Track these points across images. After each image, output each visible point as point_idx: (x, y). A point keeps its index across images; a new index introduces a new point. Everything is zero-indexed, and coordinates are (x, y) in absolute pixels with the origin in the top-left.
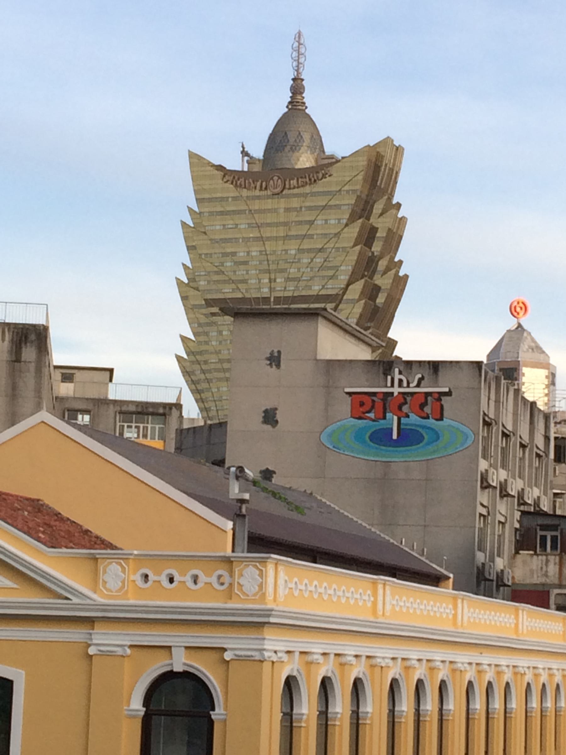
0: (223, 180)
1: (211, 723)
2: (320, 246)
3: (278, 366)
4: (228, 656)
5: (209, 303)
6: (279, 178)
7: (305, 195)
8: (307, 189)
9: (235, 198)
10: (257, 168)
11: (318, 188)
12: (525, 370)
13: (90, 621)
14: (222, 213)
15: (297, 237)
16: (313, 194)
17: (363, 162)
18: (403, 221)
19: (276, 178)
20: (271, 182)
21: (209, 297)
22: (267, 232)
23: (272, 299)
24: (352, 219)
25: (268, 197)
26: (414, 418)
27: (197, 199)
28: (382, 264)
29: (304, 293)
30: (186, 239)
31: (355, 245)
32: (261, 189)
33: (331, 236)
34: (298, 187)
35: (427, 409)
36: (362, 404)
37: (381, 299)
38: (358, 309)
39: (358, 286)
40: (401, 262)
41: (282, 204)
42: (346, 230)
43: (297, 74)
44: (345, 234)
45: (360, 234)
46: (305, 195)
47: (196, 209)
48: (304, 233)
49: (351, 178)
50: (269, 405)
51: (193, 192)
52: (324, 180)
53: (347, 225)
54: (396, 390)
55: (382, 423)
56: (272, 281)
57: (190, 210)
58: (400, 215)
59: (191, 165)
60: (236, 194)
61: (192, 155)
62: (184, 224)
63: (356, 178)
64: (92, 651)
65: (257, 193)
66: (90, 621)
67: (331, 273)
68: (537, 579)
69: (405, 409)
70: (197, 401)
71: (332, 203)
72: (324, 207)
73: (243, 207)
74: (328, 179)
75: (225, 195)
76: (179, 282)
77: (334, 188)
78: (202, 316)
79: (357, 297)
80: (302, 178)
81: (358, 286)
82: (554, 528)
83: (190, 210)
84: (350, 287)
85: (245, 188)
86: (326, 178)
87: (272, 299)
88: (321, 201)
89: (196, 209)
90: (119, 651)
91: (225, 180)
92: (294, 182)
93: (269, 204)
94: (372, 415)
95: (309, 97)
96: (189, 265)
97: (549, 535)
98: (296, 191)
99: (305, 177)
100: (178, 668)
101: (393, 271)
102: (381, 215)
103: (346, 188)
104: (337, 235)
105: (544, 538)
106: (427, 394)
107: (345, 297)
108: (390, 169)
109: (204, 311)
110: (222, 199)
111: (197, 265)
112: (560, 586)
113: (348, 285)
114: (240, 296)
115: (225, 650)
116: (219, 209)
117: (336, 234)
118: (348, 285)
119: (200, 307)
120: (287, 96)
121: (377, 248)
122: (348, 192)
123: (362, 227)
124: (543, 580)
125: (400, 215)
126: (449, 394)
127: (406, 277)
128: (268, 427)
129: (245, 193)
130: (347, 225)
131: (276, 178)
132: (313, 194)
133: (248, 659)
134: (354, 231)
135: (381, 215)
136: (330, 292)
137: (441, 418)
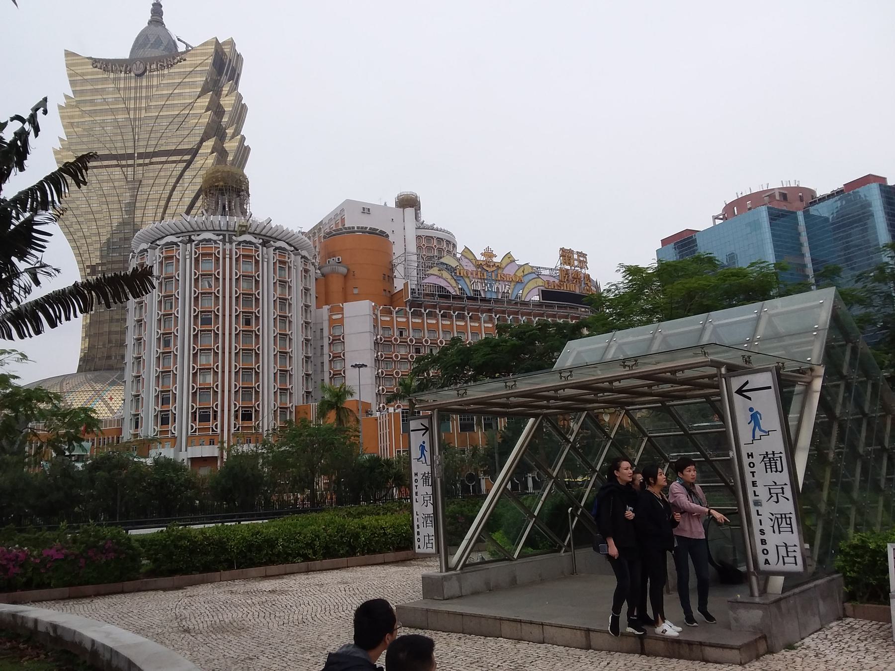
0: (93, 65)
2: (177, 113)
6: (141, 62)
7: (163, 75)
8: (166, 72)
16: (169, 74)
17: (211, 49)
19: (138, 63)
20: (134, 65)
23: (136, 155)
29: (163, 148)
32: (125, 73)
33: (186, 105)
39: (210, 144)
46: (163, 75)
48: (163, 103)
51: (69, 82)
52: (179, 63)
53: (199, 97)
56: (136, 141)
61: (68, 54)
63: (206, 61)
65: (122, 75)
70: (69, 241)
74: (183, 63)
79: (210, 151)
80: (161, 62)
83: (67, 97)
84: (204, 144)
85: (112, 72)
86: (181, 62)
87: (136, 155)
91: (94, 65)
92: (154, 66)
95: (165, 19)
98: (155, 73)
99: (163, 62)
102: (227, 95)
103: (198, 69)
108: (233, 80)
111: (69, 130)
114: (107, 152)
120: (148, 16)
129: (112, 75)
130: (199, 97)
131: (138, 63)
134: (205, 101)
135: (227, 95)
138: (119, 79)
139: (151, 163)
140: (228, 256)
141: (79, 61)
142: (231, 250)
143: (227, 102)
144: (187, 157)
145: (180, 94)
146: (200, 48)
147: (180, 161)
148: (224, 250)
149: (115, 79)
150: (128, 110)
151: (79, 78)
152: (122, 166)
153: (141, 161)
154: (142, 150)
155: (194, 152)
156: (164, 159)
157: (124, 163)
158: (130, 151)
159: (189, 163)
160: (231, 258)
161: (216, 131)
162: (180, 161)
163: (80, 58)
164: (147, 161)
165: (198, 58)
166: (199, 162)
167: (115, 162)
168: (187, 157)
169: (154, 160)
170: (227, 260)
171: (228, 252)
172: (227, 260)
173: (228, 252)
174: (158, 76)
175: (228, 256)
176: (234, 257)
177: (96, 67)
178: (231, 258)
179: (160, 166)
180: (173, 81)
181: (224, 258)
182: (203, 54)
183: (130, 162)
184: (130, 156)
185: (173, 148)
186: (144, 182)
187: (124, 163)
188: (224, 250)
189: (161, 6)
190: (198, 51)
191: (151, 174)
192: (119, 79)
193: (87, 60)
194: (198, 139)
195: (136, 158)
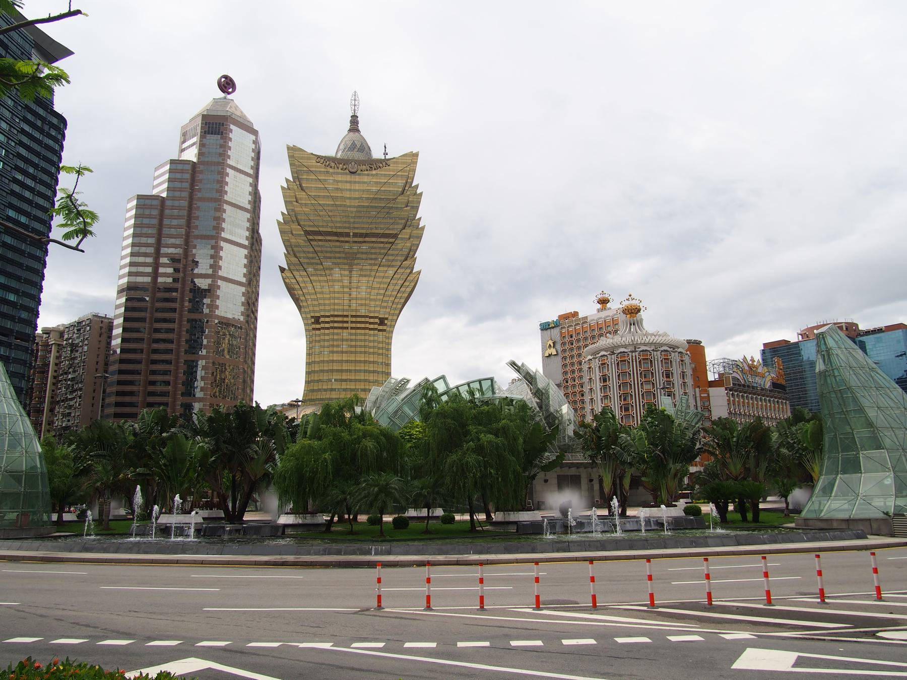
2: (383, 205)
5: (307, 233)
7: (372, 175)
8: (374, 172)
19: (353, 163)
21: (308, 229)
23: (351, 234)
29: (374, 231)
34: (367, 170)
42: (399, 198)
43: (355, 113)
49: (402, 168)
57: (287, 180)
62: (283, 188)
67: (391, 221)
77: (392, 173)
78: (302, 241)
79: (408, 237)
83: (287, 180)
86: (386, 166)
87: (351, 234)
98: (366, 172)
109: (303, 238)
117: (393, 200)
119: (300, 235)
129: (331, 170)
131: (353, 163)
139: (364, 242)
140: (634, 360)
141: (306, 156)
142: (636, 356)
146: (401, 158)
147: (387, 243)
148: (632, 356)
151: (305, 169)
153: (356, 239)
154: (356, 231)
155: (395, 236)
156: (374, 239)
158: (347, 231)
159: (393, 243)
160: (636, 361)
162: (387, 243)
163: (306, 153)
165: (399, 165)
167: (336, 238)
168: (391, 240)
169: (367, 239)
170: (634, 363)
171: (634, 358)
172: (634, 363)
173: (634, 358)
174: (368, 175)
175: (634, 360)
176: (638, 360)
177: (319, 162)
178: (636, 361)
180: (380, 181)
181: (633, 361)
182: (402, 163)
183: (347, 239)
184: (347, 235)
185: (382, 232)
188: (632, 356)
189: (357, 117)
190: (399, 160)
193: (312, 156)
194: (401, 227)
195: (351, 237)
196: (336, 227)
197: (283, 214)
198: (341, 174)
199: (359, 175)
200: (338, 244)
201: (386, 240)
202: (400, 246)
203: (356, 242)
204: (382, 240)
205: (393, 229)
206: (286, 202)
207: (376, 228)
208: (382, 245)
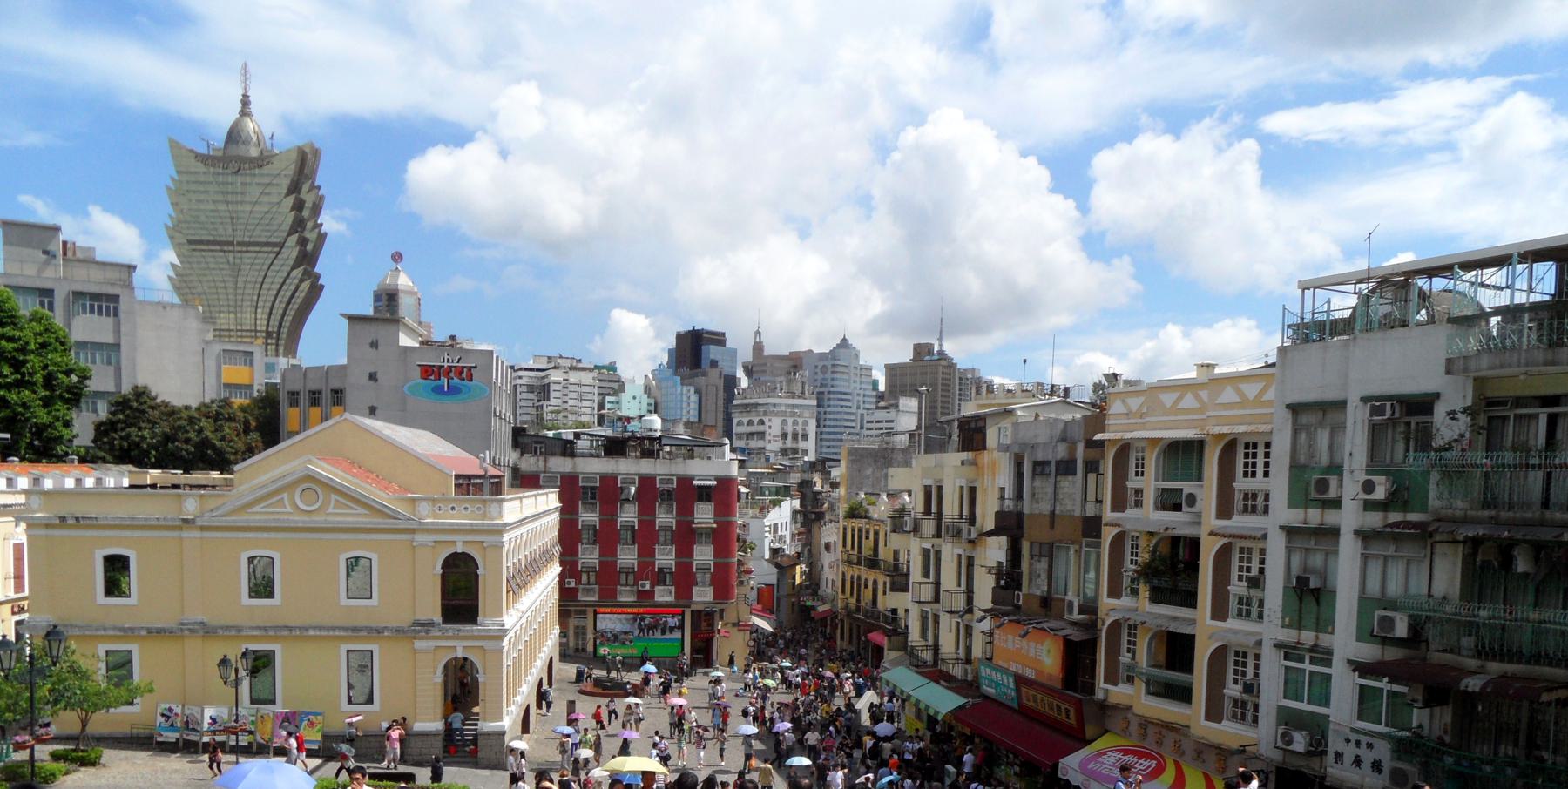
1: (477, 576)
3: (377, 348)
4: (485, 545)
7: (255, 175)
8: (257, 171)
9: (204, 173)
10: (220, 154)
11: (265, 170)
12: (401, 295)
13: (413, 531)
14: (194, 182)
15: (250, 203)
16: (262, 175)
18: (322, 198)
22: (230, 198)
24: (289, 193)
25: (228, 174)
26: (456, 381)
27: (178, 172)
28: (310, 225)
30: (170, 196)
31: (292, 210)
35: (464, 375)
36: (426, 371)
37: (309, 247)
38: (295, 253)
39: (294, 238)
40: (321, 225)
41: (239, 179)
44: (283, 204)
45: (294, 203)
46: (255, 175)
47: (176, 177)
50: (373, 371)
54: (446, 364)
55: (438, 382)
58: (320, 193)
59: (171, 147)
60: (205, 170)
64: (414, 544)
65: (221, 171)
66: (413, 531)
68: (534, 469)
69: (452, 375)
71: (275, 182)
72: (268, 185)
73: (211, 179)
75: (197, 170)
76: (167, 227)
81: (294, 238)
82: (541, 443)
88: (267, 180)
89: (176, 177)
90: (430, 544)
92: (247, 165)
93: (230, 179)
94: (432, 377)
96: (173, 215)
97: (539, 446)
100: (460, 551)
101: (317, 230)
102: (308, 192)
104: (279, 203)
105: (536, 448)
106: (463, 367)
107: (286, 244)
110: (196, 173)
112: (545, 472)
113: (288, 236)
114: (211, 238)
115: (483, 542)
116: (193, 179)
118: (288, 236)
121: (306, 213)
122: (285, 176)
123: (296, 198)
124: (535, 470)
125: (320, 193)
126: (476, 367)
127: (326, 234)
128: (372, 383)
129: (212, 169)
132: (262, 175)
133: (496, 546)
134: (291, 200)
135: (308, 192)
136: (275, 240)
137: (471, 380)
138: (218, 174)
139: (247, 251)
143: (309, 199)
144: (277, 249)
145: (269, 194)
149: (214, 174)
150: (227, 202)
152: (224, 251)
153: (239, 249)
154: (240, 239)
155: (282, 246)
156: (257, 249)
157: (226, 248)
158: (231, 239)
159: (278, 253)
161: (298, 225)
164: (244, 249)
166: (285, 252)
167: (218, 248)
168: (277, 249)
169: (249, 249)
174: (250, 175)
179: (255, 255)
183: (231, 248)
184: (231, 243)
185: (264, 240)
186: (242, 267)
187: (226, 248)
191: (249, 261)
192: (218, 174)
194: (285, 234)
196: (220, 236)
197: (170, 216)
198: (223, 174)
199: (242, 175)
200: (222, 254)
201: (270, 249)
202: (285, 256)
203: (239, 252)
204: (266, 249)
205: (277, 237)
206: (172, 204)
207: (260, 236)
208: (266, 255)
